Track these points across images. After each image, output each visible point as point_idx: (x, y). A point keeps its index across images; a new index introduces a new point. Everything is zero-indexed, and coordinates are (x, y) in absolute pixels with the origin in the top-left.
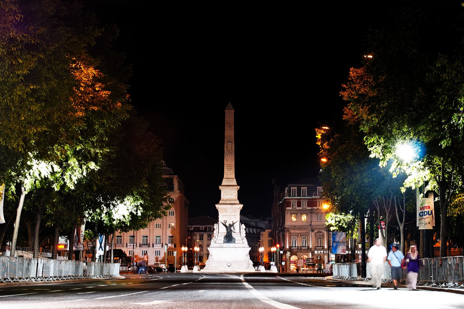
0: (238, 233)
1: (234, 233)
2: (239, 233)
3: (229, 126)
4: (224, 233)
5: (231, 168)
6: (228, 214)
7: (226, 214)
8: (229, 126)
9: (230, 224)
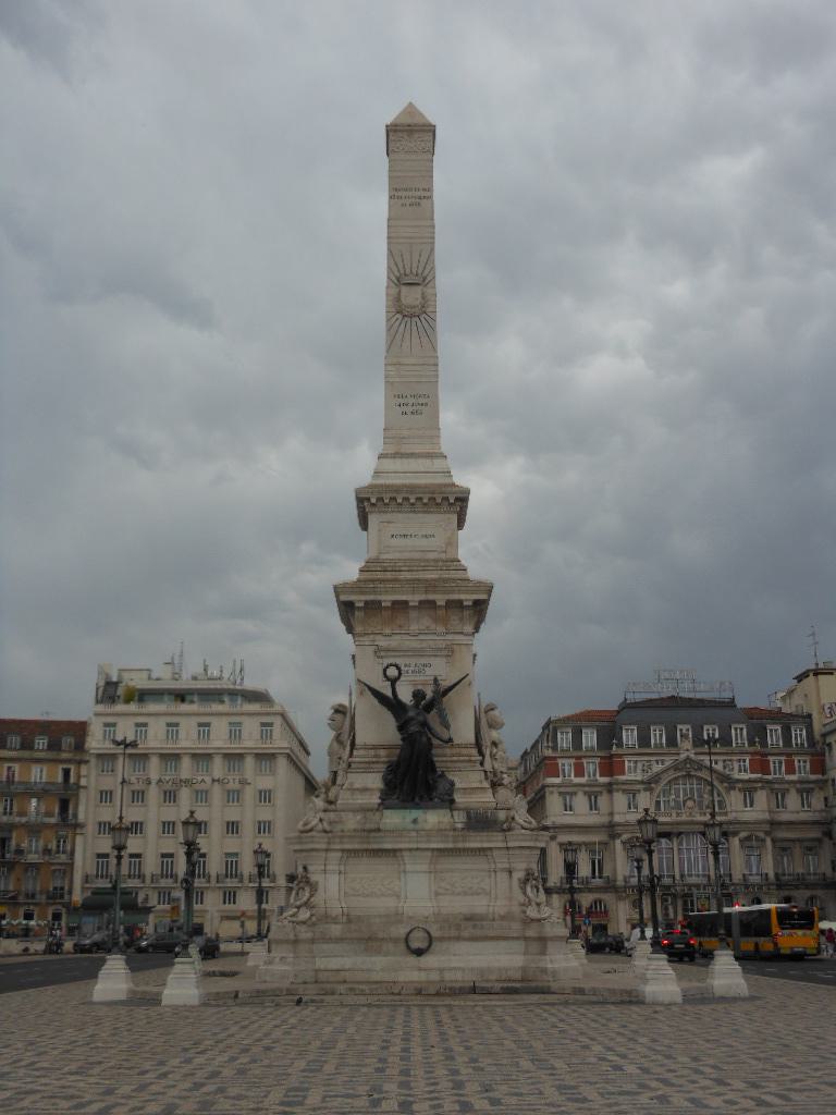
0: (466, 746)
1: (448, 751)
2: (474, 751)
3: (408, 202)
4: (382, 752)
5: (421, 401)
6: (414, 644)
7: (394, 642)
8: (408, 202)
9: (418, 695)
